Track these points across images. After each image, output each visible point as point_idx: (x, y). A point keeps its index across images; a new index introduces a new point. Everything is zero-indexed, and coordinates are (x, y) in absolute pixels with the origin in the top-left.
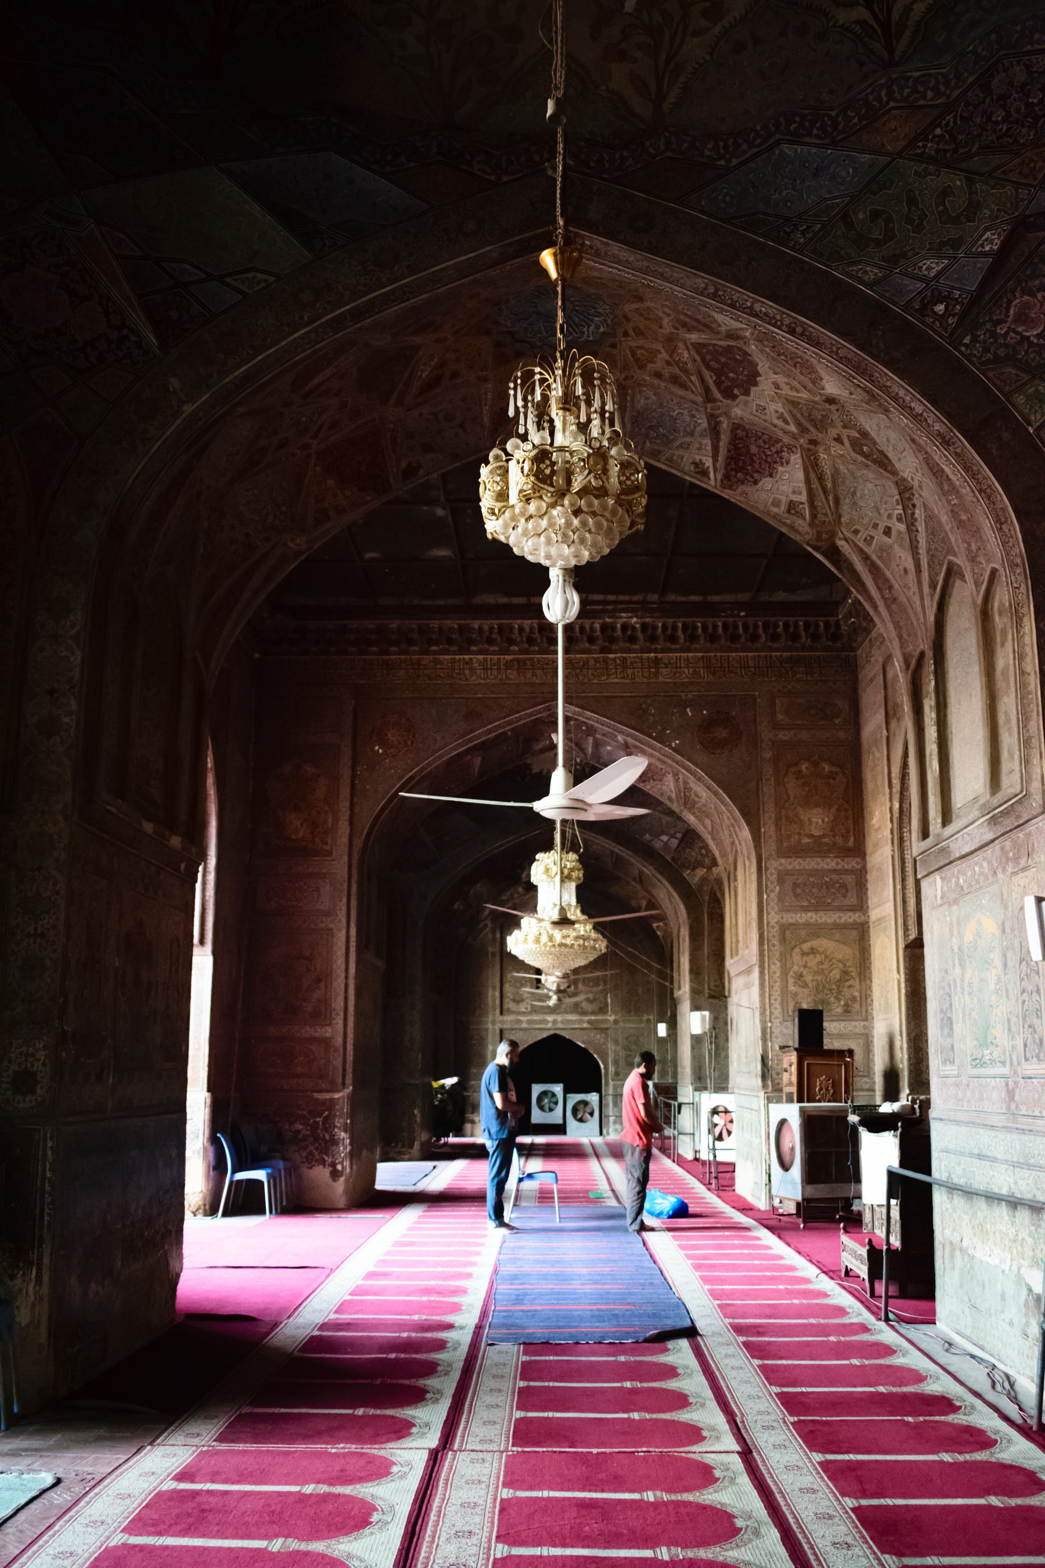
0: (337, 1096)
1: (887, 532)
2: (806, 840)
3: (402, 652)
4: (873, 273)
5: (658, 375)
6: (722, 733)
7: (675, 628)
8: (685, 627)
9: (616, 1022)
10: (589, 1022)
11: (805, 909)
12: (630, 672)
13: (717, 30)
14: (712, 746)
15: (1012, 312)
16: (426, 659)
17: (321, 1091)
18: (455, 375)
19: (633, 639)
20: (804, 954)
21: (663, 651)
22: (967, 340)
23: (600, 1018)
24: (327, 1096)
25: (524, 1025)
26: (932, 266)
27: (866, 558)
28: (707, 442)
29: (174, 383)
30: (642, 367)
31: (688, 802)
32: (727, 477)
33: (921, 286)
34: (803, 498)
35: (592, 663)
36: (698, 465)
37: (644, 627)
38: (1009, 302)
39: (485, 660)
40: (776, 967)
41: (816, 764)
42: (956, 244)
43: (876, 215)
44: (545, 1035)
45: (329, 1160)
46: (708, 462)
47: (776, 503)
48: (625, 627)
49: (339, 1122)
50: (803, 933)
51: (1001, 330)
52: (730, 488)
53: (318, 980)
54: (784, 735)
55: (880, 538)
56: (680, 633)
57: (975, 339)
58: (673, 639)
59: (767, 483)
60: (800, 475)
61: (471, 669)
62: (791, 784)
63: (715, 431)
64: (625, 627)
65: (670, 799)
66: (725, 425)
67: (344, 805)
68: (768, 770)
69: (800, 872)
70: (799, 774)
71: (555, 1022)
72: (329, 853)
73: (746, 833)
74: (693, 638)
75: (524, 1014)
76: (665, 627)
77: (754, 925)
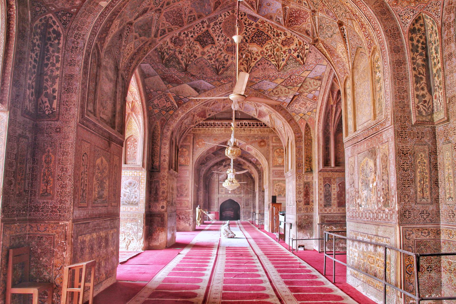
0: (190, 211)
1: (281, 128)
2: (278, 164)
6: (262, 144)
7: (254, 124)
8: (256, 124)
9: (243, 196)
11: (277, 177)
13: (256, 62)
14: (261, 146)
16: (207, 129)
19: (246, 126)
20: (277, 186)
21: (252, 128)
23: (240, 195)
24: (188, 211)
26: (284, 99)
27: (279, 130)
28: (255, 112)
29: (180, 112)
31: (257, 155)
32: (258, 117)
34: (270, 121)
37: (248, 123)
40: (272, 188)
41: (280, 150)
42: (287, 96)
43: (277, 91)
44: (228, 199)
45: (189, 222)
46: (256, 114)
47: (266, 121)
49: (190, 215)
50: (277, 181)
51: (293, 108)
53: (186, 189)
54: (274, 144)
55: (280, 128)
56: (255, 124)
58: (254, 126)
59: (264, 118)
60: (269, 118)
62: (275, 154)
63: (256, 110)
66: (258, 110)
67: (191, 157)
68: (271, 151)
69: (276, 170)
70: (277, 152)
71: (230, 196)
72: (188, 166)
73: (267, 163)
74: (258, 126)
75: (223, 194)
76: (252, 124)
77: (268, 180)
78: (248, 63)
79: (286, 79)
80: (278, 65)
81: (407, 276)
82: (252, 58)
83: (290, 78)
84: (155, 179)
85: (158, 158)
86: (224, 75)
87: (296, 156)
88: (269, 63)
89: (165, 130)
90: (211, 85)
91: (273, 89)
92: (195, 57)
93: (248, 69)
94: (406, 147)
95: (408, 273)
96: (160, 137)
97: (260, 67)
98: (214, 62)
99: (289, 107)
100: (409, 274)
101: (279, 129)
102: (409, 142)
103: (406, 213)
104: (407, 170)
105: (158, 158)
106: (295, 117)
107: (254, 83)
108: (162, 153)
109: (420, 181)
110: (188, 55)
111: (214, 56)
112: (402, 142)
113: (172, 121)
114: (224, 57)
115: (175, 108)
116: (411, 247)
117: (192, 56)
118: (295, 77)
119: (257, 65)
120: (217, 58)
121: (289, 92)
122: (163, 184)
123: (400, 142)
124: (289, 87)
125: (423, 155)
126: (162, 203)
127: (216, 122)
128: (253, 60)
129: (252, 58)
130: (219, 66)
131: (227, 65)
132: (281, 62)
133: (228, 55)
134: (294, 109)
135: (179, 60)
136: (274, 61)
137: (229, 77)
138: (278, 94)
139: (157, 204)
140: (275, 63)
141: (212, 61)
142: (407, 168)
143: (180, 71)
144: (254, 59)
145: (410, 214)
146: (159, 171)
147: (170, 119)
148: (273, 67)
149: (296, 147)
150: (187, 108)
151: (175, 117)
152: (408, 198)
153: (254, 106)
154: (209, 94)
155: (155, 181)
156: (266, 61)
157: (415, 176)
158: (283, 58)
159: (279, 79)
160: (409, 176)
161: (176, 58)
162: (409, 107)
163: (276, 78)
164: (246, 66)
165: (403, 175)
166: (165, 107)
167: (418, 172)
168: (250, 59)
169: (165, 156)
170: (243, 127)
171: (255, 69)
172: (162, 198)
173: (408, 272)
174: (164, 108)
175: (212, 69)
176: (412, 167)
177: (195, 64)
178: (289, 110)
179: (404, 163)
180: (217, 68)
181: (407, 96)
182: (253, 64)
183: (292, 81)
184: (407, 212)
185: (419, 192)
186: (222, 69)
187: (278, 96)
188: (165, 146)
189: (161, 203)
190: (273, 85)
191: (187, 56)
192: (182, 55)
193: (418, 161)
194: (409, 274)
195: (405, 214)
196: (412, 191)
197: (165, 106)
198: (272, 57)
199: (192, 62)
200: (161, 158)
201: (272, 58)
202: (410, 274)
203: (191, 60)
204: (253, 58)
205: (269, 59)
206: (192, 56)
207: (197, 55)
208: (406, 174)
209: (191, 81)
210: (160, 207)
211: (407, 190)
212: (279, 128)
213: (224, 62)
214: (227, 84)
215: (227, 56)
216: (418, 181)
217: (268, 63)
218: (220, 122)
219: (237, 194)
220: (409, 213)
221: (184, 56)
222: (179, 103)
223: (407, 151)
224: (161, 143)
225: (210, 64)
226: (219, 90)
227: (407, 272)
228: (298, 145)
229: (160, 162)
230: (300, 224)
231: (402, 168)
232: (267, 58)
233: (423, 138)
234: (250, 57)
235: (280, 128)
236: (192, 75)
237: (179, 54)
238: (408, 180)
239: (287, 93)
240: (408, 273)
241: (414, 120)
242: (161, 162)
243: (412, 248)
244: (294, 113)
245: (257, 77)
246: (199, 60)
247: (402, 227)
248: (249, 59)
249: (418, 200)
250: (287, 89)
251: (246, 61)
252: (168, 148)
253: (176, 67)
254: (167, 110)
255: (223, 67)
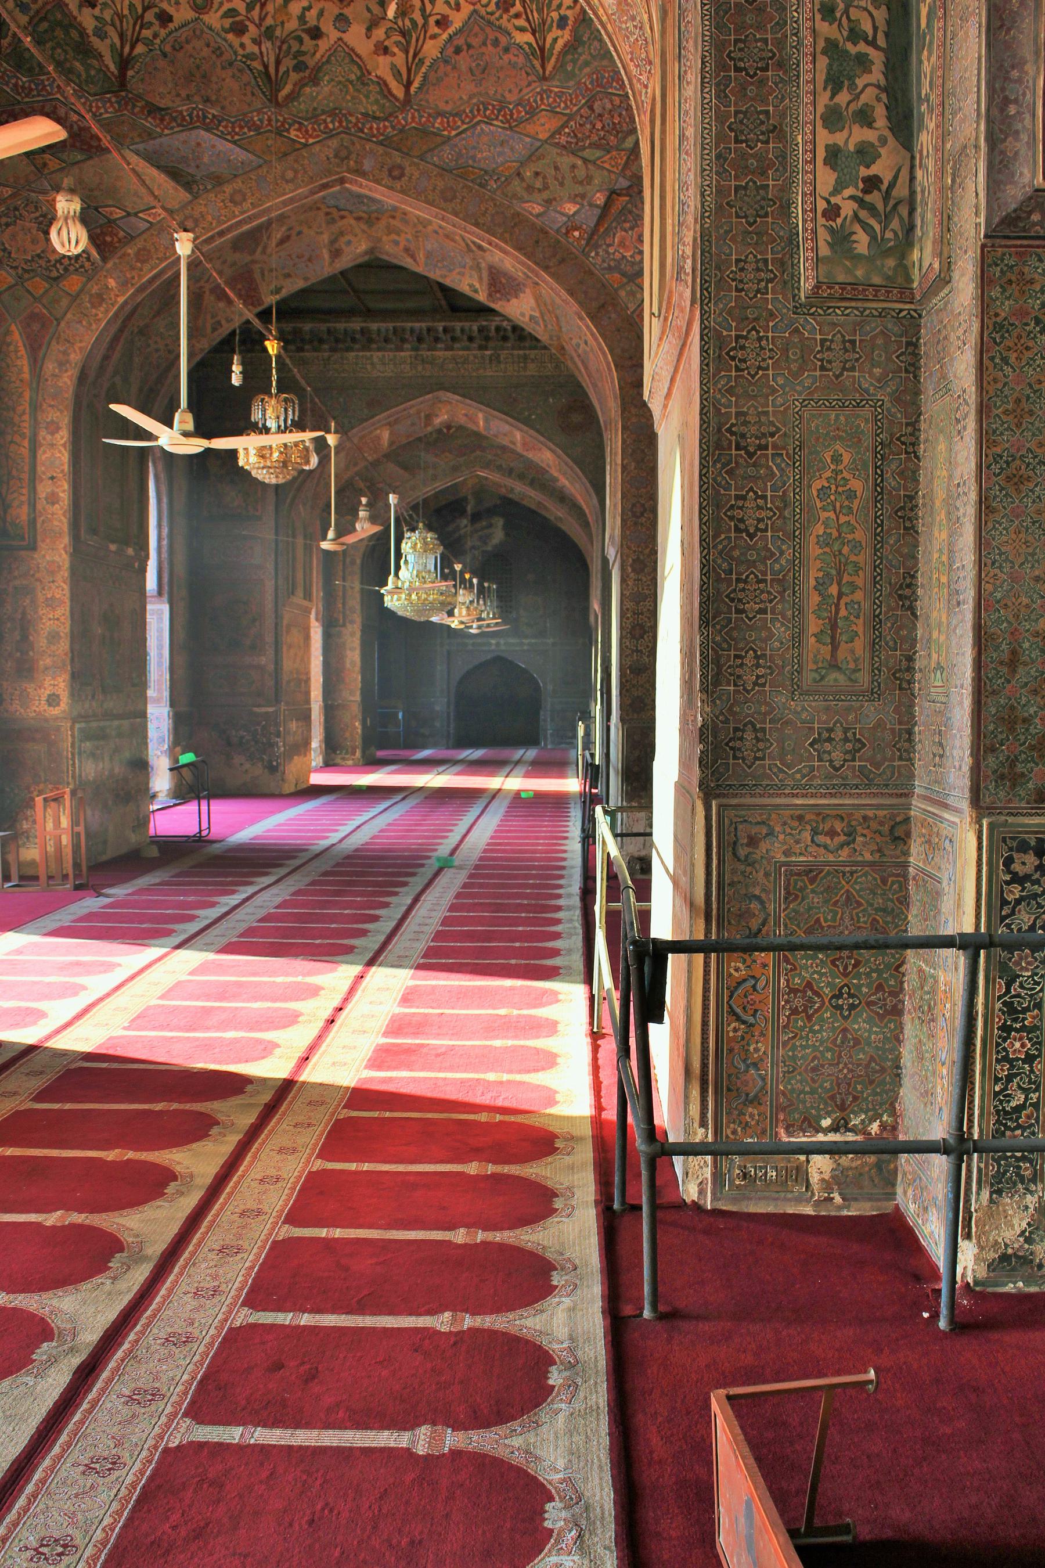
3: (315, 350)
4: (538, 209)
5: (436, 232)
10: (529, 644)
12: (502, 366)
13: (445, 36)
15: (616, 240)
17: (259, 706)
18: (299, 233)
21: (531, 348)
22: (593, 254)
24: (263, 710)
25: (470, 648)
26: (571, 208)
29: (112, 283)
30: (425, 227)
32: (490, 295)
33: (565, 219)
35: (471, 358)
36: (471, 286)
38: (614, 235)
39: (384, 356)
42: (583, 196)
43: (537, 174)
44: (489, 657)
47: (523, 315)
48: (498, 329)
51: (611, 250)
52: (493, 302)
53: (254, 620)
57: (597, 254)
59: (514, 301)
61: (372, 364)
63: (478, 267)
64: (498, 329)
65: (548, 465)
71: (498, 644)
78: (408, 43)
79: (570, 117)
80: (542, 49)
81: (735, 1030)
82: (426, 17)
83: (591, 108)
84: (17, 582)
85: (25, 491)
86: (301, 106)
87: (624, 468)
88: (504, 40)
89: (50, 367)
90: (239, 155)
91: (522, 164)
92: (165, 18)
93: (409, 70)
94: (759, 414)
95: (738, 1019)
96: (27, 395)
97: (463, 61)
98: (254, 41)
99: (596, 247)
100: (744, 1022)
101: (580, 351)
102: (774, 391)
103: (741, 739)
104: (757, 529)
105: (25, 491)
106: (622, 293)
107: (439, 140)
108: (40, 469)
109: (821, 586)
110: (126, 12)
111: (256, 13)
112: (739, 391)
113: (80, 322)
114: (302, 18)
115: (87, 264)
116: (758, 898)
117: (149, 16)
118: (609, 106)
119: (450, 50)
120: (269, 21)
121: (589, 179)
122: (51, 603)
123: (730, 391)
124: (587, 153)
125: (846, 458)
126: (48, 682)
127: (374, 326)
128: (434, 30)
129: (426, 17)
130: (278, 62)
131: (318, 55)
132: (555, 32)
133: (321, 5)
134: (618, 256)
135: (82, 33)
136: (522, 30)
137: (324, 112)
138: (546, 187)
139: (30, 688)
140: (528, 37)
141: (246, 39)
142: (759, 520)
143: (93, 89)
144: (438, 23)
145: (761, 745)
146: (33, 547)
147: (69, 316)
148: (521, 60)
149: (624, 428)
150: (143, 262)
151: (93, 306)
152: (758, 666)
153: (465, 250)
154: (238, 198)
155: (15, 588)
156: (488, 30)
157: (798, 563)
158: (562, 12)
159: (543, 118)
160: (766, 558)
161: (71, 25)
162: (789, 215)
163: (532, 112)
164: (400, 59)
165: (736, 553)
166: (43, 263)
167: (813, 539)
168: (420, 21)
169: (52, 478)
170: (491, 344)
171: (440, 73)
172: (48, 661)
173: (738, 1010)
174: (35, 266)
175: (247, 77)
176: (786, 513)
177: (165, 55)
178: (595, 259)
179: (743, 498)
180: (272, 70)
181: (783, 156)
182: (431, 49)
183: (599, 126)
184: (749, 735)
185: (813, 640)
186: (294, 77)
187: (546, 195)
188: (52, 434)
189: (47, 684)
190: (520, 146)
191: (121, 17)
192: (97, 11)
193: (817, 485)
194: (744, 1022)
195: (738, 744)
196: (779, 630)
197: (39, 256)
198: (513, 11)
199: (148, 43)
200: (40, 488)
201: (517, 16)
202: (751, 1020)
203: (147, 33)
204: (432, 21)
205: (504, 22)
206: (149, 16)
207: (171, 10)
208: (750, 548)
209: (150, 135)
210: (44, 699)
211: (750, 628)
212: (578, 345)
213: (301, 41)
214: (317, 148)
215: (314, 12)
216: (813, 583)
217: (496, 43)
218: (391, 326)
219: (526, 637)
220: (758, 740)
221: (107, 15)
222: (105, 242)
223: (764, 435)
224: (36, 424)
225: (235, 53)
226: (283, 177)
227: (732, 1012)
228: (634, 420)
229: (33, 504)
230: (636, 769)
231: (731, 518)
232: (492, 18)
233: (853, 369)
234: (417, 16)
235: (583, 345)
236: (153, 110)
237: (80, 6)
238: (759, 581)
239: (581, 183)
240: (738, 1019)
241: (807, 279)
242: (39, 507)
243: (762, 903)
244: (617, 275)
245: (448, 108)
246: (184, 34)
247: (719, 806)
248: (414, 23)
249: (809, 677)
250: (580, 162)
251: (403, 33)
252: (64, 445)
253: (71, 71)
254: (55, 274)
255: (300, 67)
